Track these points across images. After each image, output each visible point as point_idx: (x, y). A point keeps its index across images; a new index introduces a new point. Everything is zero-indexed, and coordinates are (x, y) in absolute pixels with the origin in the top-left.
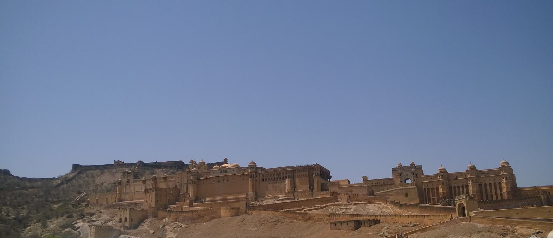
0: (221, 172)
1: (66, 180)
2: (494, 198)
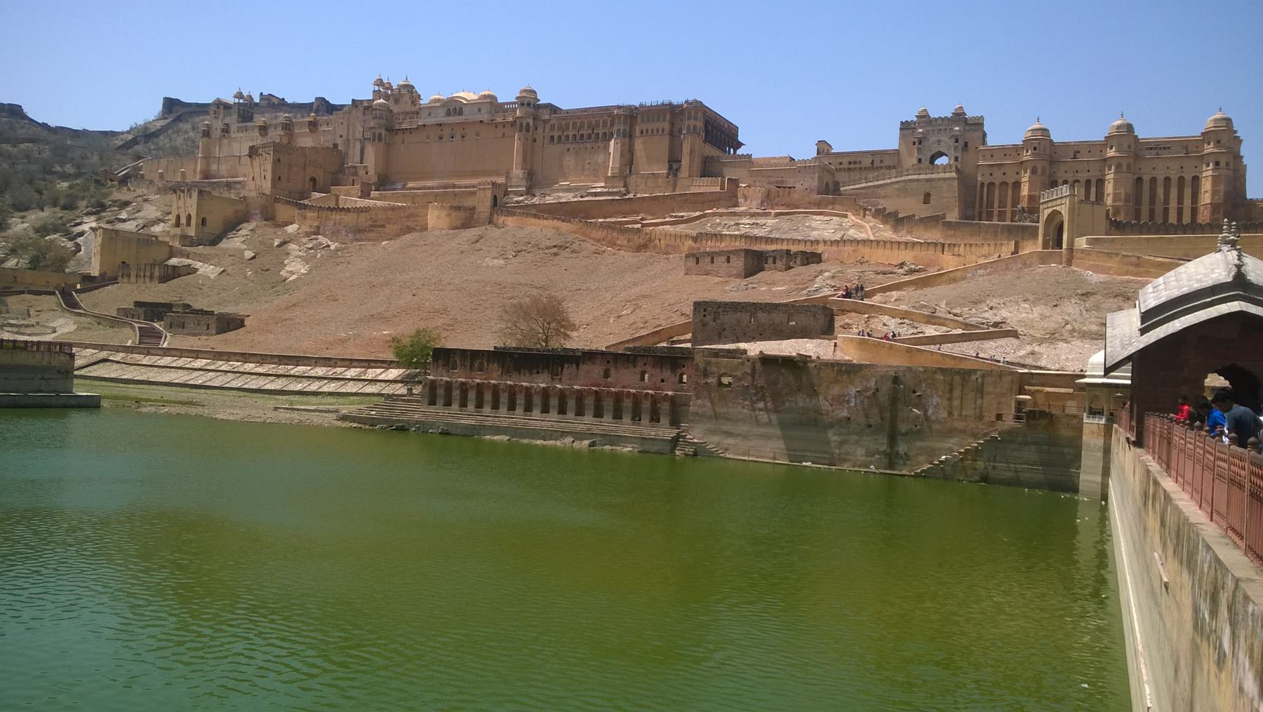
0: (448, 114)
1: (145, 135)
2: (1173, 219)
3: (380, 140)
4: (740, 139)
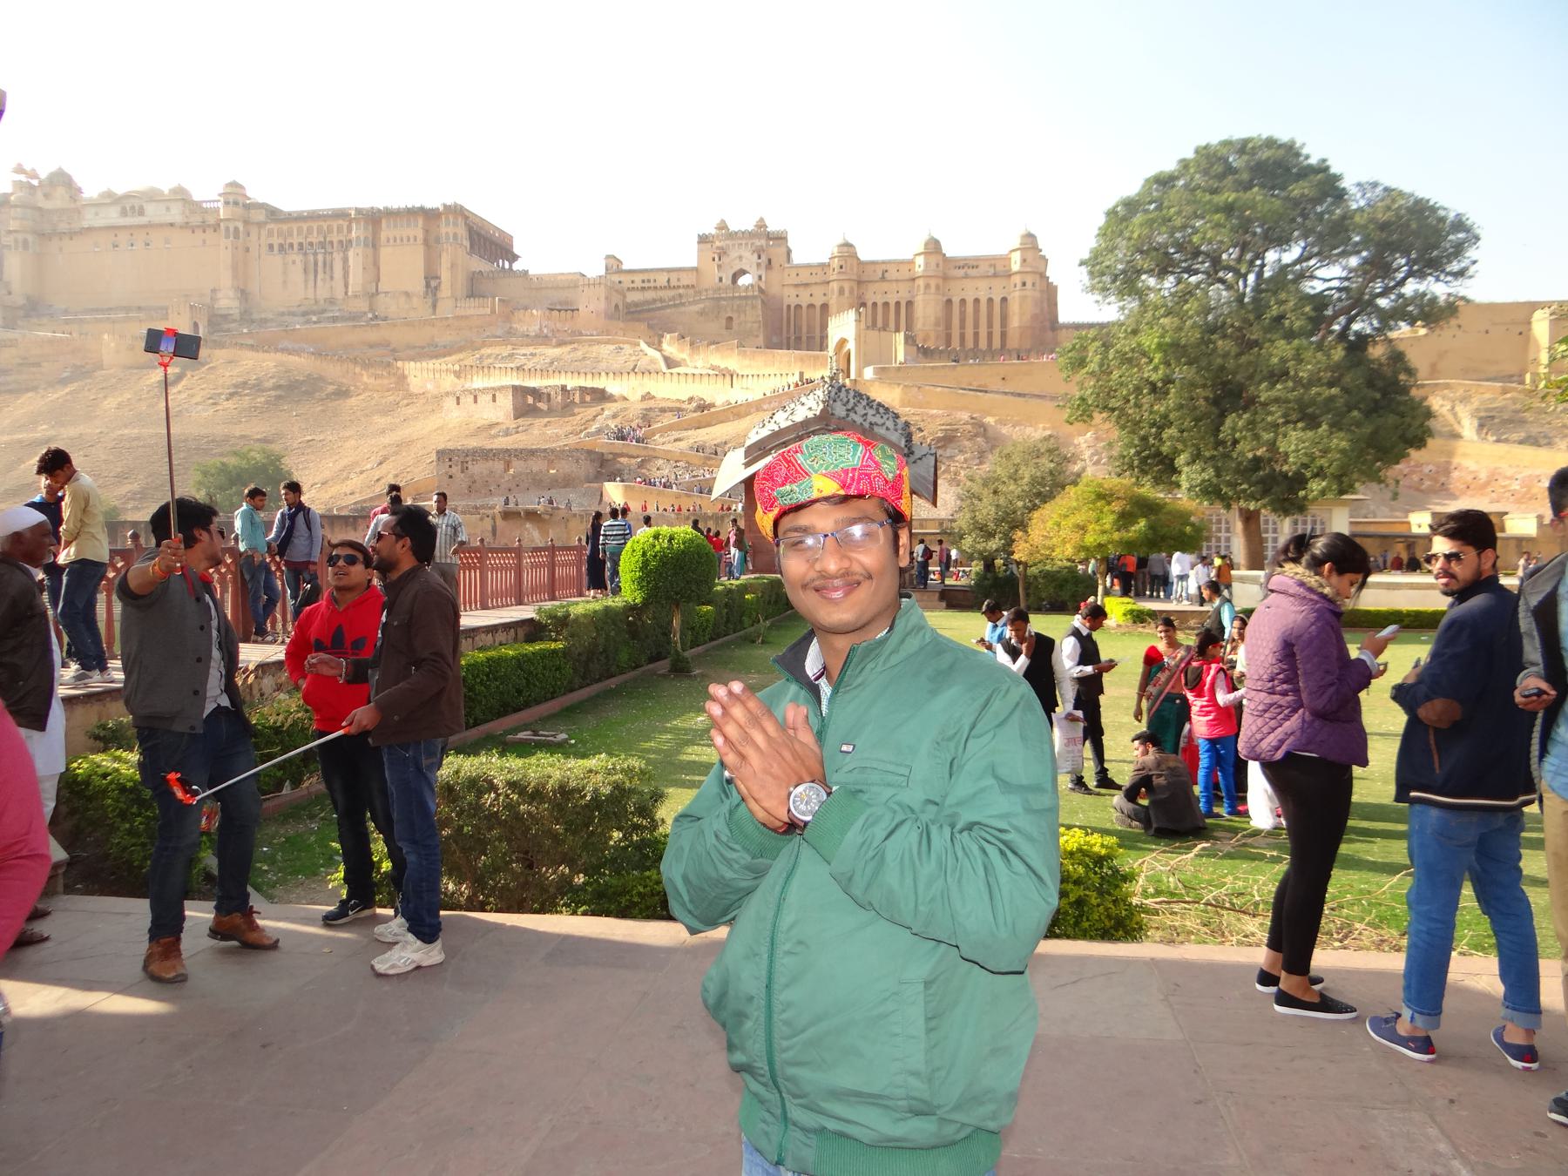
2: (983, 344)
4: (516, 250)
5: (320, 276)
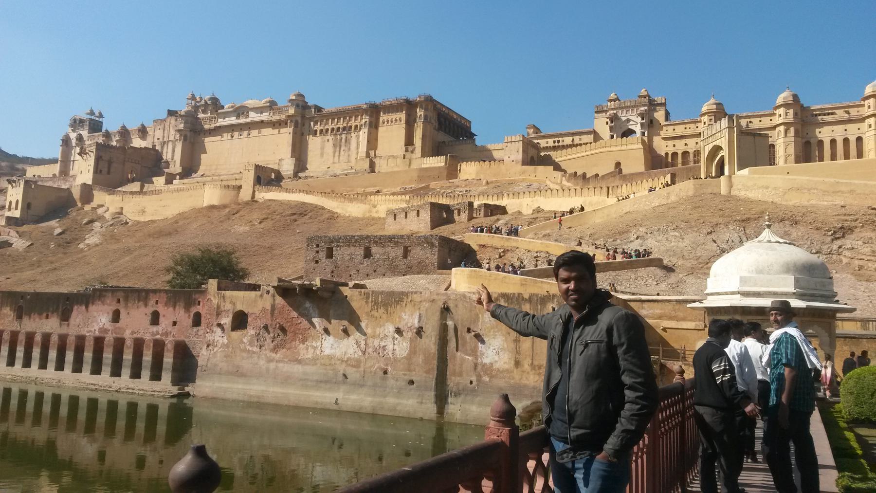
0: (238, 116)
3: (185, 139)
4: (473, 130)
5: (343, 148)
